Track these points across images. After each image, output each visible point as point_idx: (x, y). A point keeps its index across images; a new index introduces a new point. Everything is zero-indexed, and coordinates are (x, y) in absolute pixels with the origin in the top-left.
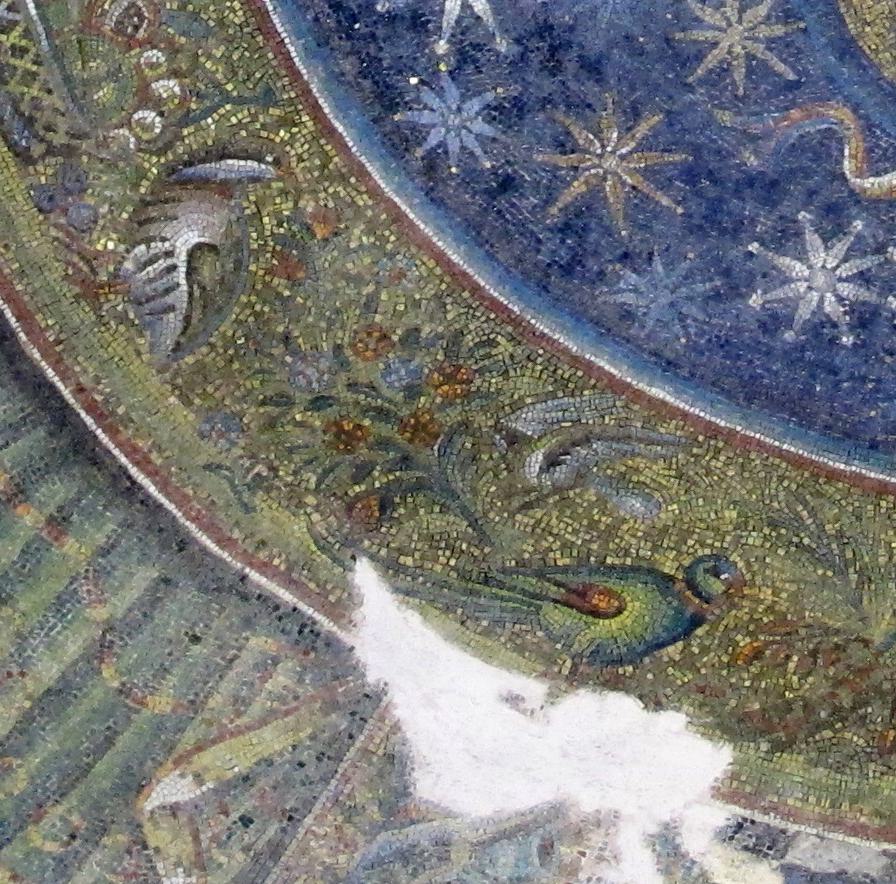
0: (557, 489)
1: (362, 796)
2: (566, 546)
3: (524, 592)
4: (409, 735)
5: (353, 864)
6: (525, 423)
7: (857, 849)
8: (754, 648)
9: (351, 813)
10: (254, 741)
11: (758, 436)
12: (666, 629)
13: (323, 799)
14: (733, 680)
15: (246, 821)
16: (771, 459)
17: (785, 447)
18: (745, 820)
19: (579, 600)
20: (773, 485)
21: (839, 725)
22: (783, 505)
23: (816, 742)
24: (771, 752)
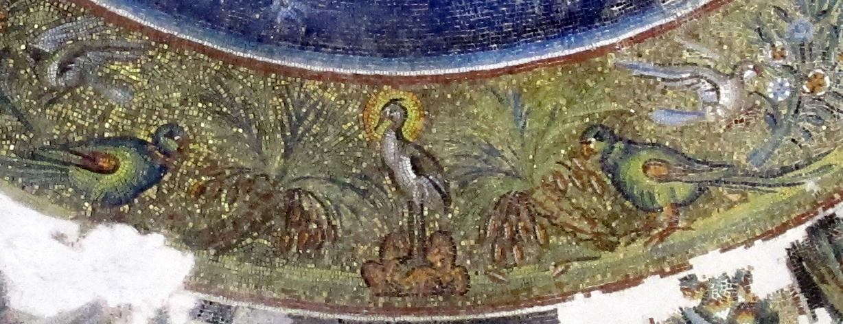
0: (69, 89)
2: (80, 127)
3: (56, 161)
6: (44, 44)
7: (273, 314)
8: (200, 186)
11: (188, 37)
12: (145, 178)
14: (189, 209)
16: (198, 55)
17: (205, 44)
18: (206, 302)
19: (91, 164)
20: (201, 72)
21: (256, 234)
22: (208, 85)
23: (243, 247)
24: (216, 255)
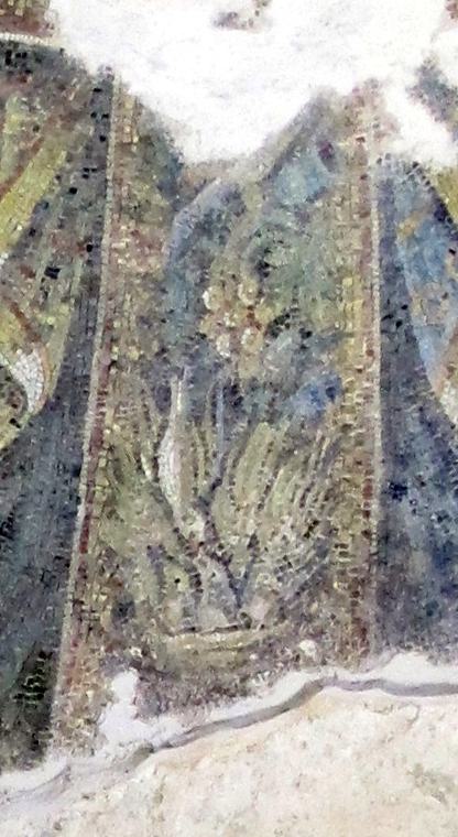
1: (141, 191)
4: (153, 107)
5: (165, 260)
9: (138, 213)
10: (22, 191)
13: (108, 212)
15: (52, 272)
